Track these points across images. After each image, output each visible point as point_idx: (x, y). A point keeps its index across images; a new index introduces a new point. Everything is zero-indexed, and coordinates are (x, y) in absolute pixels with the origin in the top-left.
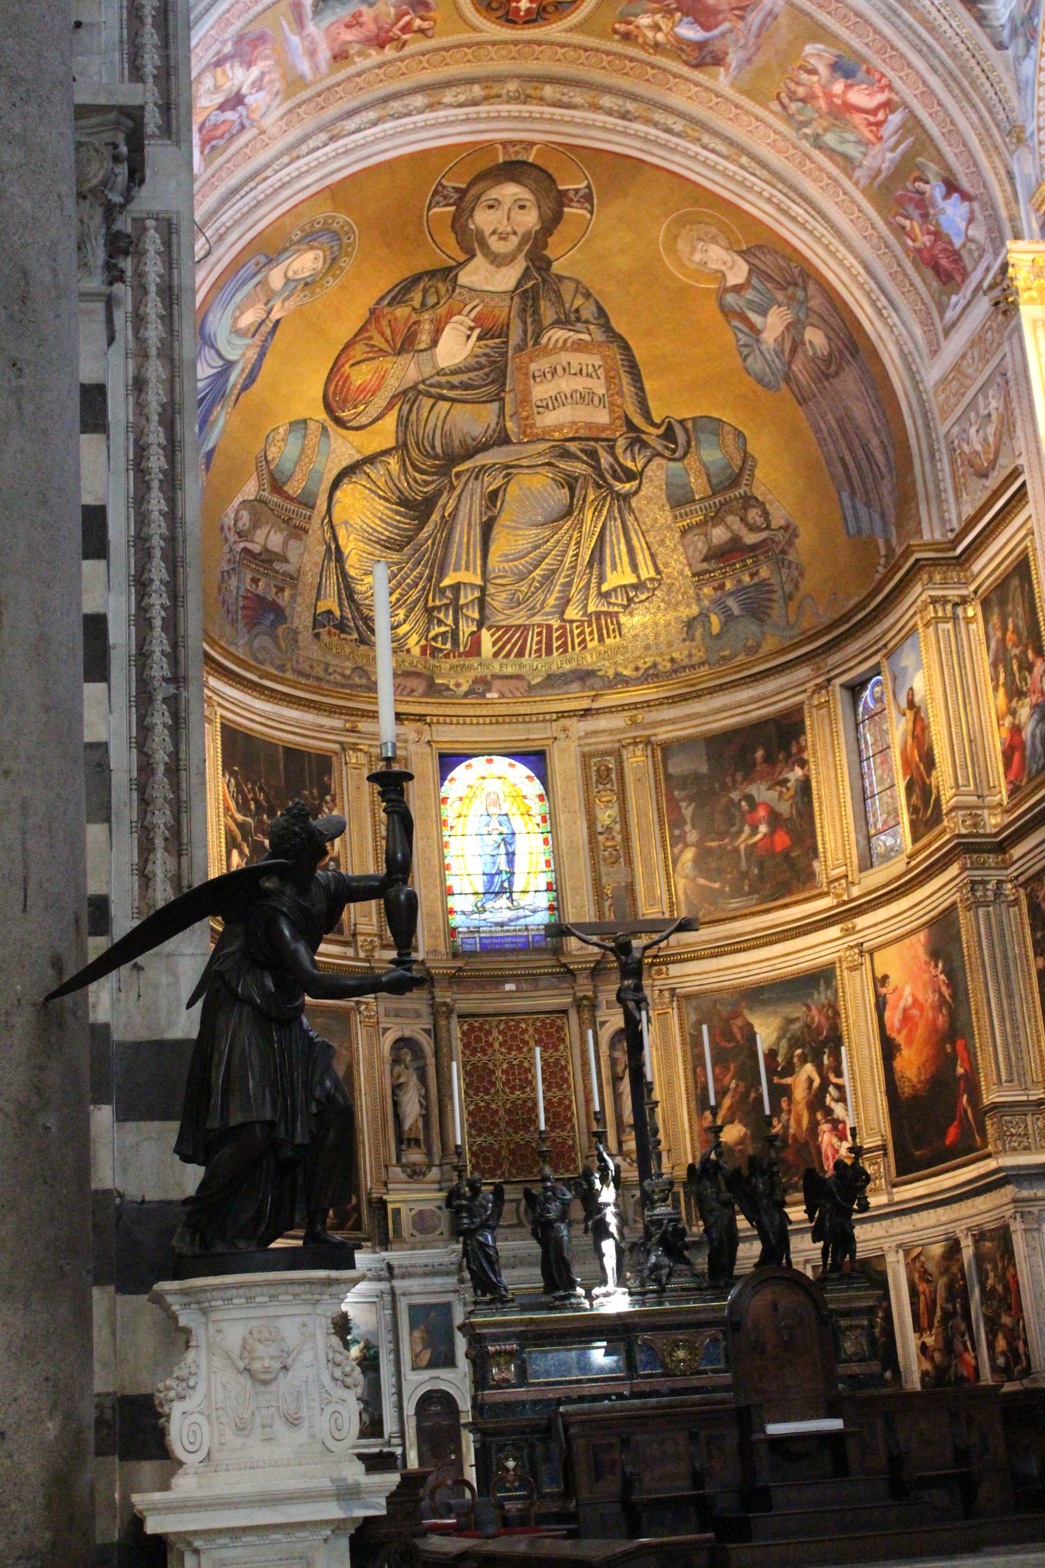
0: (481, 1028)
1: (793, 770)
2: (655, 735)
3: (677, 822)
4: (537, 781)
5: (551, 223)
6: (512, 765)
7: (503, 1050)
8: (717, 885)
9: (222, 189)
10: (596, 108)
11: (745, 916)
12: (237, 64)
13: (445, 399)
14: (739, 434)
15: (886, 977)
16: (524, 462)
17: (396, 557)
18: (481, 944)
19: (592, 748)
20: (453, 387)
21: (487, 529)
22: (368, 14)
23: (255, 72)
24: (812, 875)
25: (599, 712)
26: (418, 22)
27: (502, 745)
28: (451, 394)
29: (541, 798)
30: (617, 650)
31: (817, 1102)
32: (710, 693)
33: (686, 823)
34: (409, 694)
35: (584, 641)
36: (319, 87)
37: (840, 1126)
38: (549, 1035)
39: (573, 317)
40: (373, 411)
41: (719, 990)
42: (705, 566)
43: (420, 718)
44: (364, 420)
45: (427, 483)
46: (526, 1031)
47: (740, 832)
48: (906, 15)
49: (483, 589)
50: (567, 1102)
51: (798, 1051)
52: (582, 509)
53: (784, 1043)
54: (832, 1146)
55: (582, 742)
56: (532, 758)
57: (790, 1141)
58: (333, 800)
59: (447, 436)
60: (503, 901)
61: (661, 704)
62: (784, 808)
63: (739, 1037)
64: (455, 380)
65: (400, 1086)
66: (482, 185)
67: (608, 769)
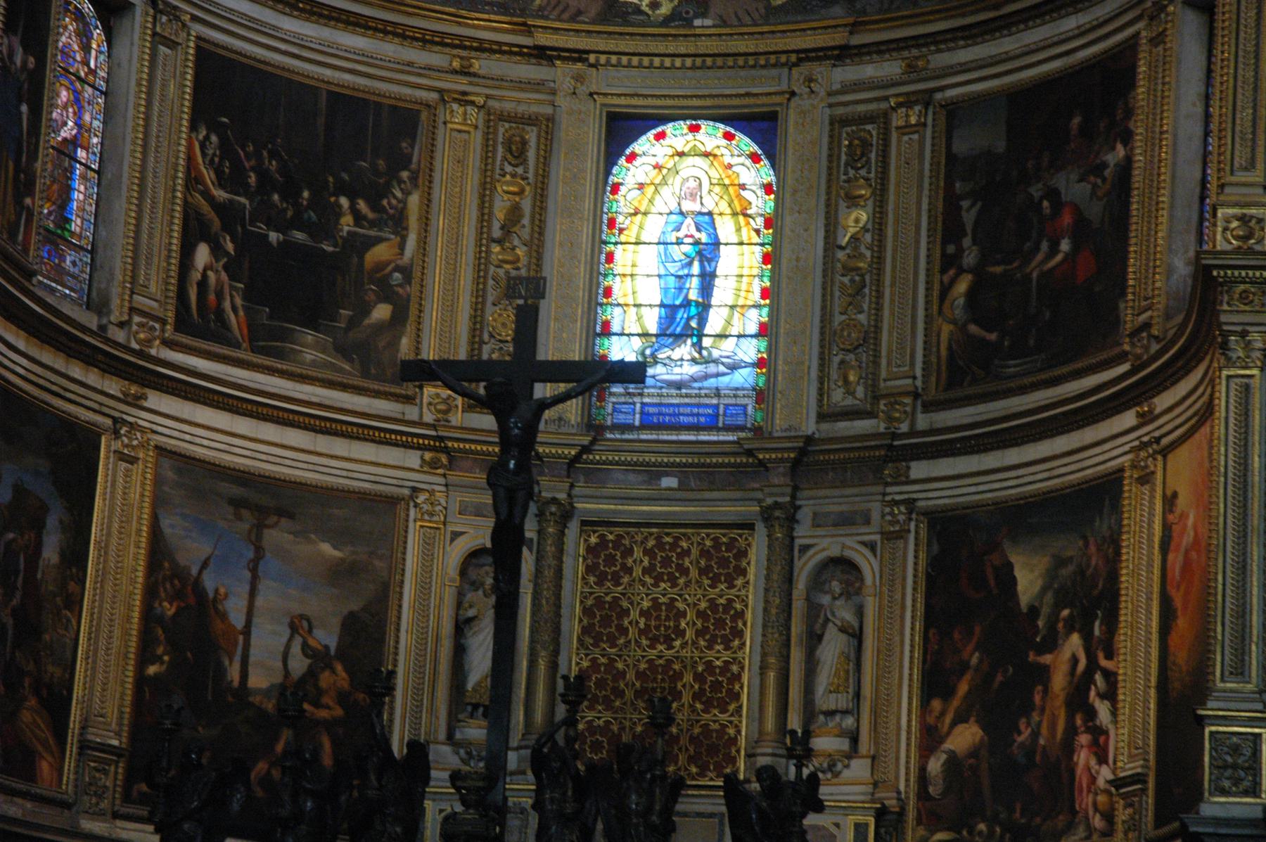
0: (617, 543)
1: (1113, 148)
2: (942, 89)
4: (765, 162)
6: (729, 137)
7: (649, 580)
8: (993, 337)
11: (1023, 390)
15: (1175, 495)
18: (642, 413)
19: (850, 109)
24: (1115, 322)
27: (709, 102)
29: (768, 189)
32: (1025, 21)
33: (965, 235)
34: (573, 19)
37: (1102, 739)
38: (724, 562)
41: (978, 505)
46: (687, 553)
47: (1037, 248)
50: (735, 668)
51: (1066, 612)
53: (1049, 598)
54: (1089, 769)
55: (833, 100)
56: (764, 125)
57: (1038, 758)
58: (414, 179)
60: (685, 350)
61: (953, 40)
62: (1095, 211)
63: (992, 582)
65: (469, 621)
67: (866, 145)
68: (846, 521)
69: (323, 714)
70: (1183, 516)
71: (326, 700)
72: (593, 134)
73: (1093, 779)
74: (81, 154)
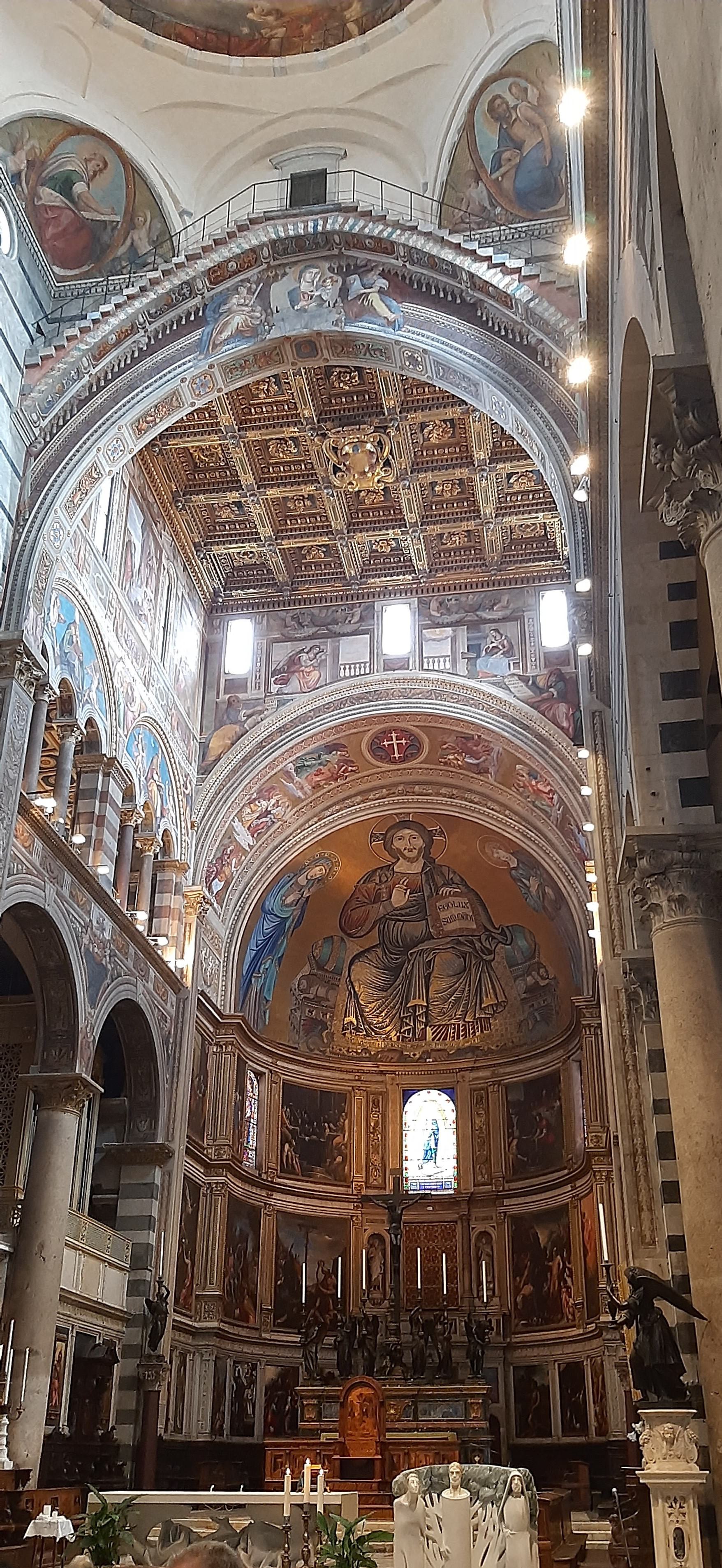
3: (510, 1125)
5: (430, 843)
9: (271, 847)
10: (438, 794)
12: (261, 800)
13: (400, 920)
14: (531, 932)
16: (441, 947)
17: (385, 994)
20: (403, 916)
21: (428, 978)
22: (324, 769)
23: (273, 801)
25: (478, 1068)
26: (350, 768)
28: (403, 918)
30: (489, 1036)
31: (561, 1277)
35: (474, 1032)
36: (310, 800)
39: (450, 882)
40: (366, 929)
42: (524, 996)
43: (394, 1073)
44: (362, 934)
45: (397, 959)
48: (551, 753)
49: (427, 1007)
52: (470, 969)
59: (404, 938)
64: (403, 912)
66: (393, 831)
68: (485, 1219)
69: (329, 1292)
70: (587, 1221)
71: (330, 1288)
72: (399, 1096)
73: (568, 1303)
74: (252, 1120)
